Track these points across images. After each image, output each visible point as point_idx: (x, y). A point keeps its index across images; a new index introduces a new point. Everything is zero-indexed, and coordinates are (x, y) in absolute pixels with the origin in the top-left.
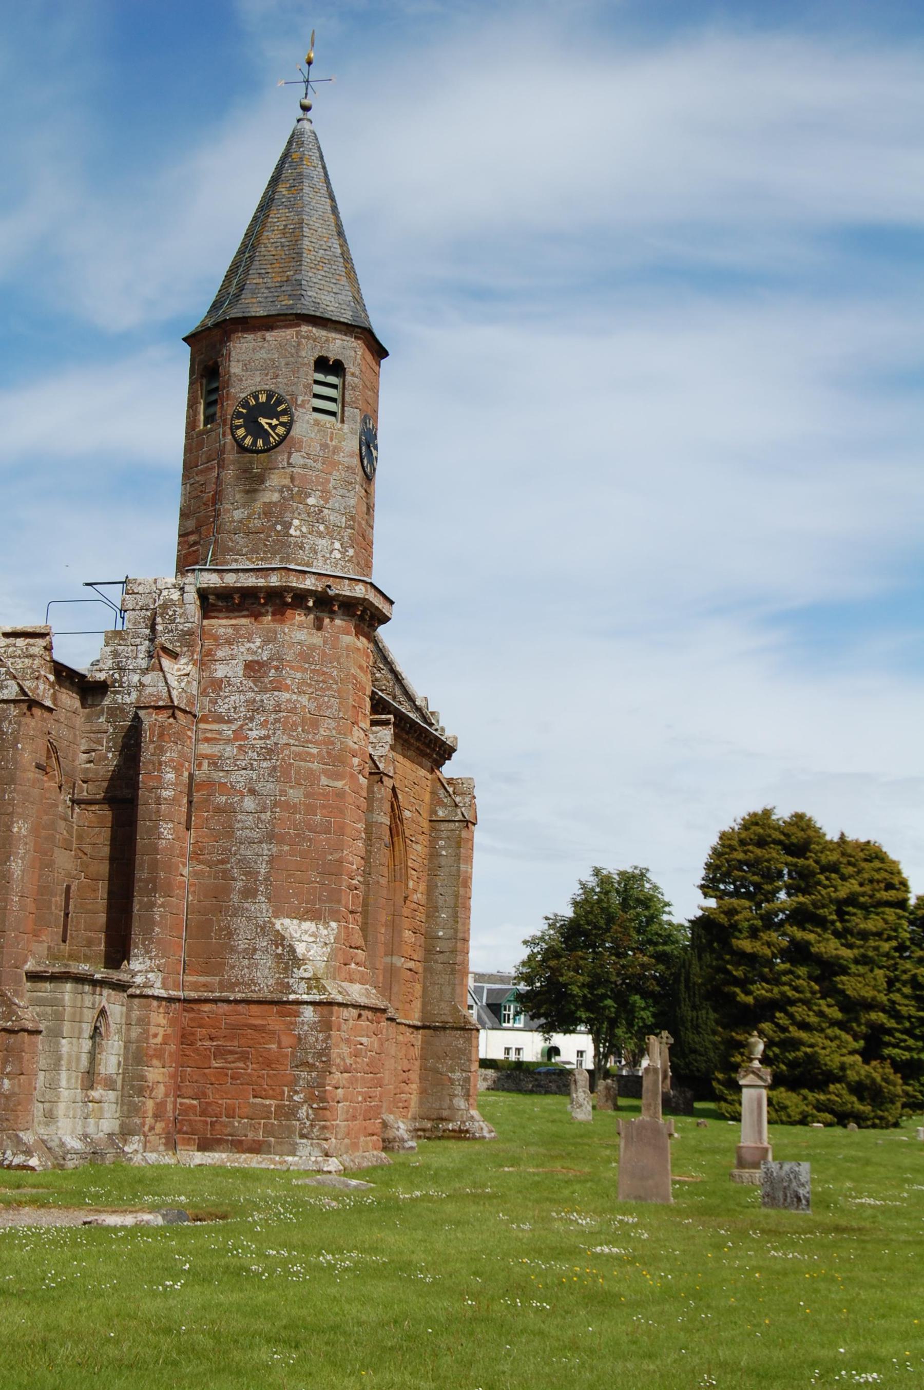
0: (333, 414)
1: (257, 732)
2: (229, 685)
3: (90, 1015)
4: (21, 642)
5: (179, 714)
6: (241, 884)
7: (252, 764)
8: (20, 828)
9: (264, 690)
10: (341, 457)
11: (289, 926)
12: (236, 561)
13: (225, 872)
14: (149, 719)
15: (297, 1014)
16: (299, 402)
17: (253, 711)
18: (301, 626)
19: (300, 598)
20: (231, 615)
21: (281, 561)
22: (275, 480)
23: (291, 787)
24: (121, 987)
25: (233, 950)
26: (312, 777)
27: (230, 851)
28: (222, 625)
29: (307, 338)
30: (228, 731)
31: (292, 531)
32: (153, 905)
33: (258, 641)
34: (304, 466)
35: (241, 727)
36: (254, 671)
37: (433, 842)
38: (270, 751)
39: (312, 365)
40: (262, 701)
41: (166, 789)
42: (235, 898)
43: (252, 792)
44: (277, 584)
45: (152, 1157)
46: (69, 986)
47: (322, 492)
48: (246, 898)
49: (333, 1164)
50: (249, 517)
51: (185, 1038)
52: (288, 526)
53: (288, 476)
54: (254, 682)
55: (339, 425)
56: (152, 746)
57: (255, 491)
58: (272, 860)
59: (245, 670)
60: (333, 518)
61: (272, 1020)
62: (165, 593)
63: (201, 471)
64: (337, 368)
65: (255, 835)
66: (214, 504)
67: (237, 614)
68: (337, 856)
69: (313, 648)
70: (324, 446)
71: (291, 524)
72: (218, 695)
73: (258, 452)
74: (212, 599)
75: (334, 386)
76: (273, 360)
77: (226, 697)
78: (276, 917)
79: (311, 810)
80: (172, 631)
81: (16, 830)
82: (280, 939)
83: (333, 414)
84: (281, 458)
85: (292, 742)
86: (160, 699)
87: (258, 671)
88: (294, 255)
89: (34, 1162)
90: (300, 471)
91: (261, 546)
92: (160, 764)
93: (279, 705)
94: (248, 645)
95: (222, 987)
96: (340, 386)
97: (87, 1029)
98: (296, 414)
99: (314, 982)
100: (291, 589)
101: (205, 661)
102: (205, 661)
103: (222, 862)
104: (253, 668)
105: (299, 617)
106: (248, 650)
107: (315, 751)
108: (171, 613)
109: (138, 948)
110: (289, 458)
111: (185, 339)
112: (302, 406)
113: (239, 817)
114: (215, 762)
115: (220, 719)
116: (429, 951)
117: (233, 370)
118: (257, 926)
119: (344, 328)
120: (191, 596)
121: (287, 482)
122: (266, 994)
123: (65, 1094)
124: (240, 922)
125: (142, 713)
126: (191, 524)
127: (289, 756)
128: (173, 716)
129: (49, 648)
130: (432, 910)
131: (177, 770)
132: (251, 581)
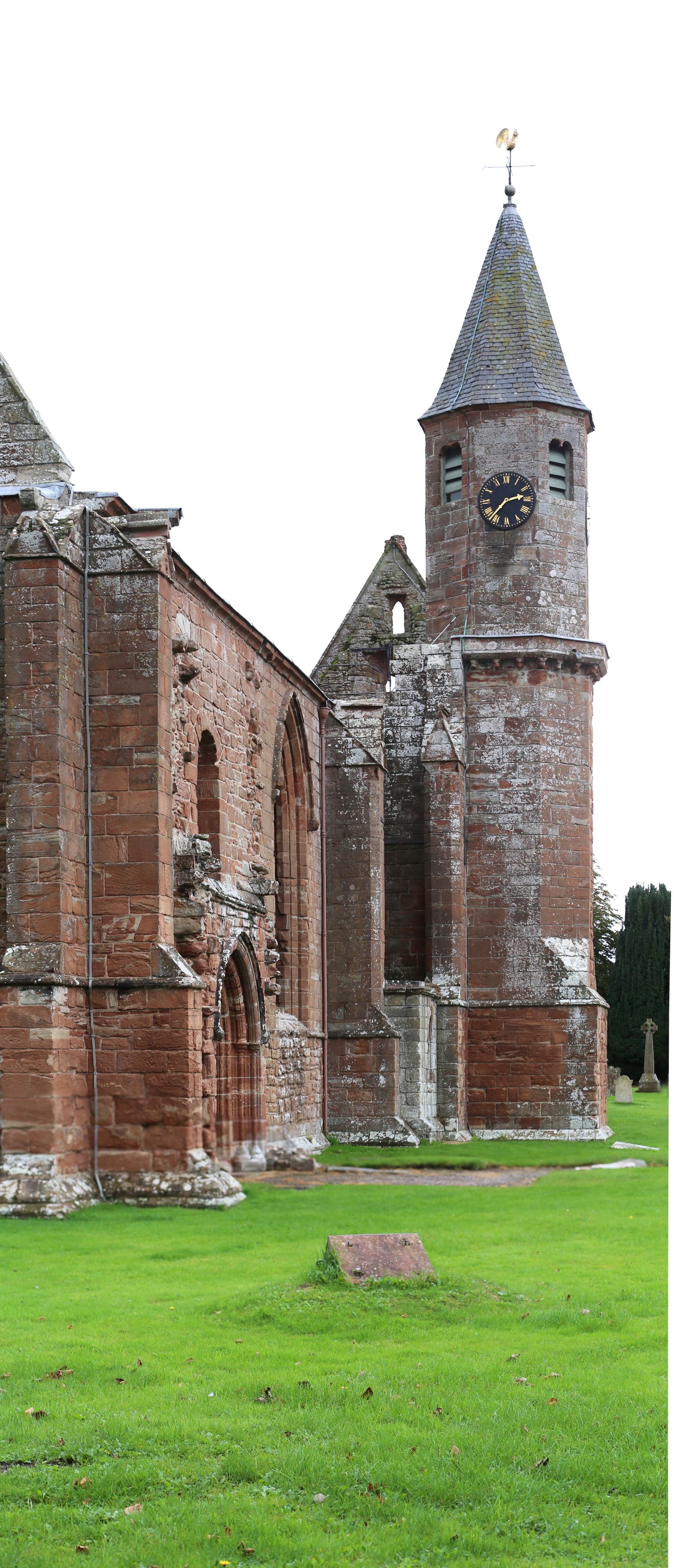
0: (562, 491)
1: (520, 780)
2: (493, 739)
5: (459, 765)
6: (514, 910)
7: (516, 808)
8: (375, 873)
9: (525, 743)
12: (491, 628)
13: (498, 900)
14: (434, 772)
16: (540, 483)
17: (515, 761)
18: (551, 687)
19: (552, 661)
20: (491, 677)
21: (533, 627)
22: (520, 555)
23: (550, 827)
26: (564, 816)
27: (501, 882)
29: (543, 423)
30: (493, 779)
31: (540, 602)
32: (448, 930)
33: (516, 700)
34: (546, 542)
35: (506, 775)
36: (514, 726)
39: (548, 449)
40: (523, 753)
41: (454, 832)
42: (508, 923)
44: (534, 650)
47: (561, 564)
48: (518, 921)
50: (500, 590)
52: (536, 597)
53: (534, 552)
54: (515, 736)
55: (570, 503)
56: (439, 796)
57: (505, 565)
59: (505, 726)
62: (430, 659)
63: (448, 545)
64: (560, 447)
66: (466, 575)
67: (496, 677)
69: (560, 704)
71: (539, 595)
72: (483, 748)
73: (505, 529)
74: (474, 663)
75: (562, 466)
76: (514, 445)
77: (490, 750)
78: (544, 937)
80: (442, 693)
81: (372, 874)
83: (562, 491)
84: (527, 536)
85: (550, 787)
86: (444, 754)
87: (518, 727)
88: (522, 343)
90: (544, 546)
91: (512, 615)
92: (448, 810)
93: (538, 757)
94: (507, 704)
95: (501, 996)
96: (567, 467)
98: (538, 495)
100: (542, 654)
103: (496, 892)
105: (551, 677)
106: (508, 708)
107: (566, 794)
108: (439, 677)
109: (438, 966)
110: (534, 535)
111: (420, 421)
112: (542, 487)
113: (507, 854)
115: (486, 769)
117: (477, 454)
118: (528, 944)
119: (570, 412)
120: (457, 662)
121: (533, 557)
125: (428, 767)
127: (547, 800)
128: (457, 770)
132: (511, 648)
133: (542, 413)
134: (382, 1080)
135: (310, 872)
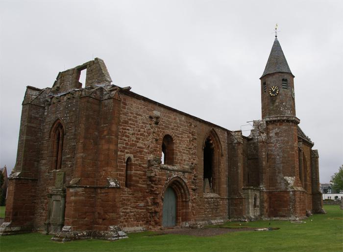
3: (253, 195)
4: (237, 133)
6: (277, 172)
9: (279, 137)
10: (288, 96)
11: (287, 178)
15: (289, 193)
22: (277, 101)
24: (259, 190)
25: (277, 183)
26: (288, 152)
28: (270, 127)
30: (273, 145)
33: (277, 129)
37: (311, 162)
38: (281, 148)
42: (277, 174)
43: (278, 155)
45: (266, 219)
46: (250, 190)
49: (297, 219)
51: (270, 198)
58: (283, 167)
60: (288, 106)
61: (286, 195)
64: (286, 80)
65: (279, 163)
68: (294, 165)
70: (285, 94)
79: (289, 157)
82: (285, 180)
84: (278, 97)
89: (246, 220)
97: (253, 198)
99: (292, 188)
101: (268, 134)
102: (268, 134)
104: (276, 134)
105: (284, 124)
114: (271, 151)
115: (271, 143)
116: (312, 180)
120: (265, 122)
122: (284, 190)
123: (250, 208)
124: (278, 178)
126: (264, 110)
129: (241, 133)
130: (312, 173)
131: (265, 152)
132: (275, 119)
133: (280, 74)
134: (241, 207)
135: (222, 165)
